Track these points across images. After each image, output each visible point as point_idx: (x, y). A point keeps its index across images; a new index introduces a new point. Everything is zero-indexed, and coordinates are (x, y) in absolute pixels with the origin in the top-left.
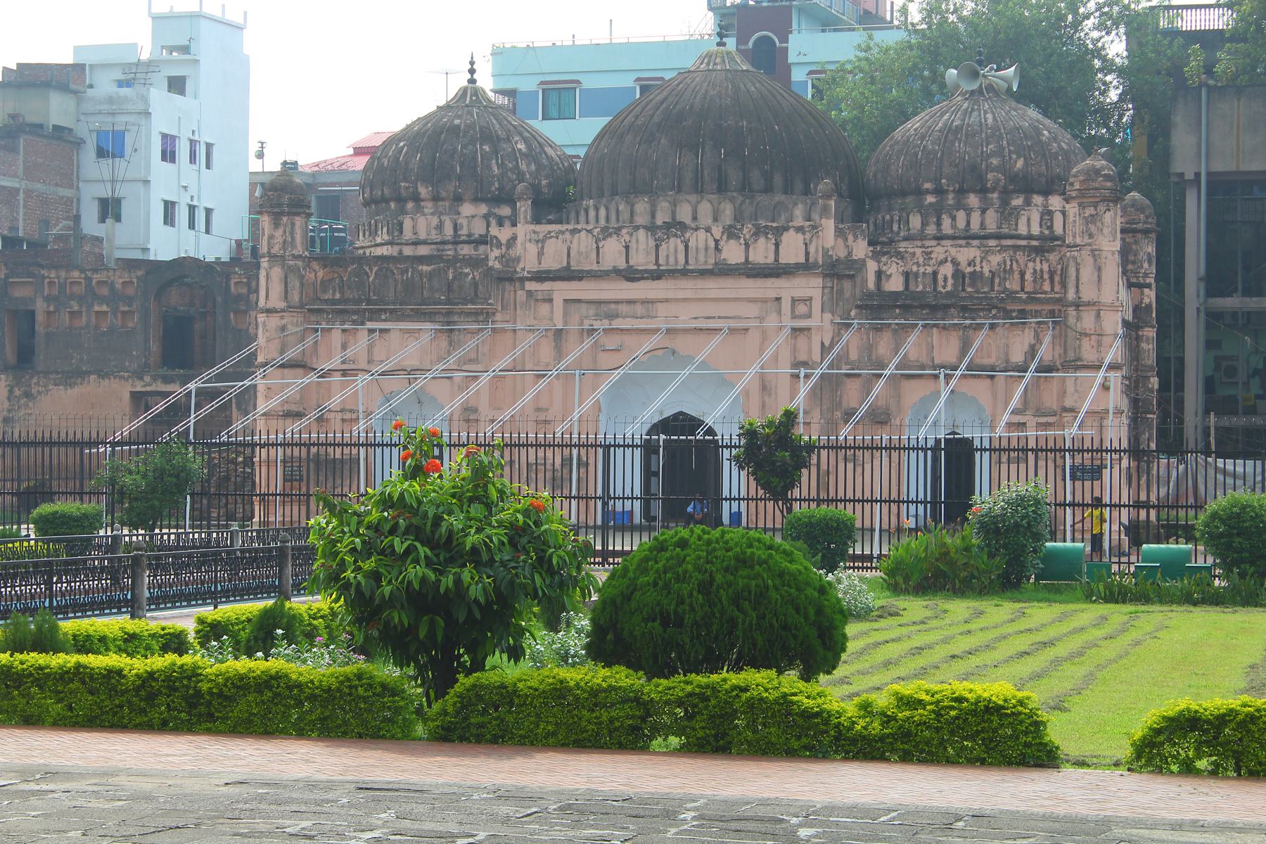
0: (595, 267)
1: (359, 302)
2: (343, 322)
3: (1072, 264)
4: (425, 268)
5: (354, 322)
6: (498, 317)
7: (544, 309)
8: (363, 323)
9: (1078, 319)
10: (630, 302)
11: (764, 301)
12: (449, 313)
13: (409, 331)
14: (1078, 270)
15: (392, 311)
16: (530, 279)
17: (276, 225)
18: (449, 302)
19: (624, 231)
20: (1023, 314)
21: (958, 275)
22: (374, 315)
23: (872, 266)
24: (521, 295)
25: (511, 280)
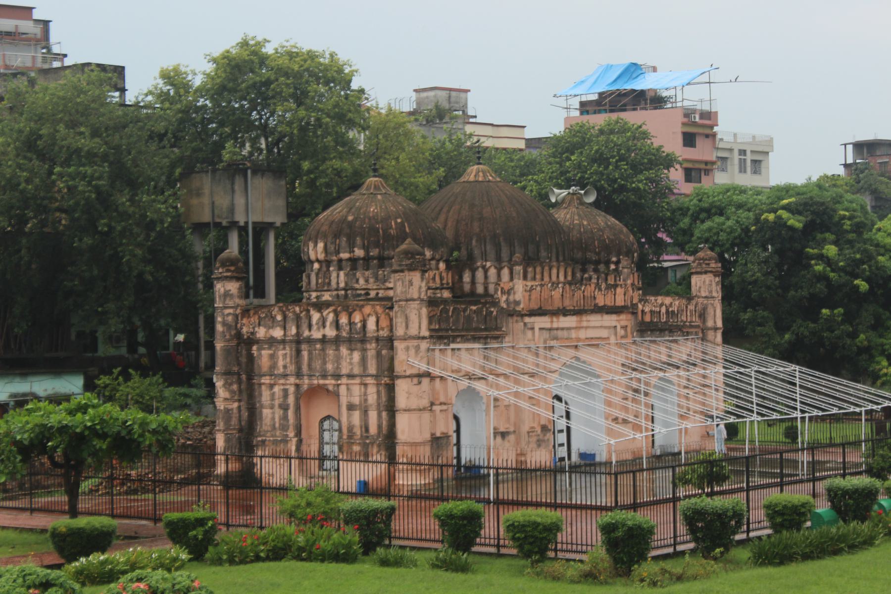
0: (551, 308)
1: (447, 330)
2: (440, 344)
3: (710, 306)
4: (474, 308)
5: (445, 344)
6: (507, 339)
7: (529, 334)
8: (449, 345)
9: (716, 337)
10: (563, 329)
11: (609, 327)
12: (486, 338)
13: (467, 349)
14: (715, 311)
15: (462, 336)
16: (526, 315)
17: (422, 279)
18: (486, 330)
19: (560, 285)
20: (688, 334)
21: (667, 312)
22: (454, 339)
23: (640, 306)
24: (522, 324)
25: (512, 315)
